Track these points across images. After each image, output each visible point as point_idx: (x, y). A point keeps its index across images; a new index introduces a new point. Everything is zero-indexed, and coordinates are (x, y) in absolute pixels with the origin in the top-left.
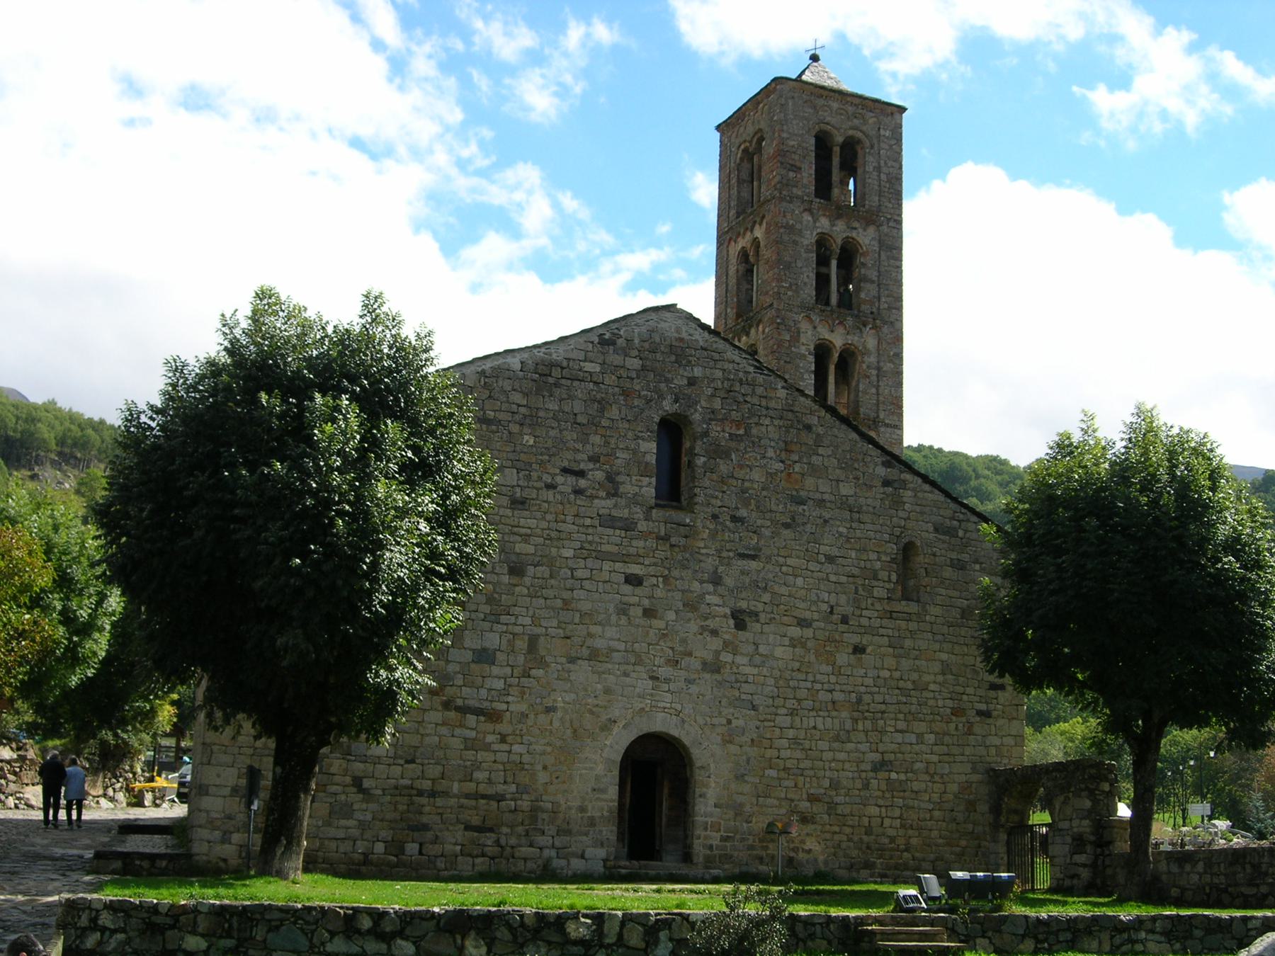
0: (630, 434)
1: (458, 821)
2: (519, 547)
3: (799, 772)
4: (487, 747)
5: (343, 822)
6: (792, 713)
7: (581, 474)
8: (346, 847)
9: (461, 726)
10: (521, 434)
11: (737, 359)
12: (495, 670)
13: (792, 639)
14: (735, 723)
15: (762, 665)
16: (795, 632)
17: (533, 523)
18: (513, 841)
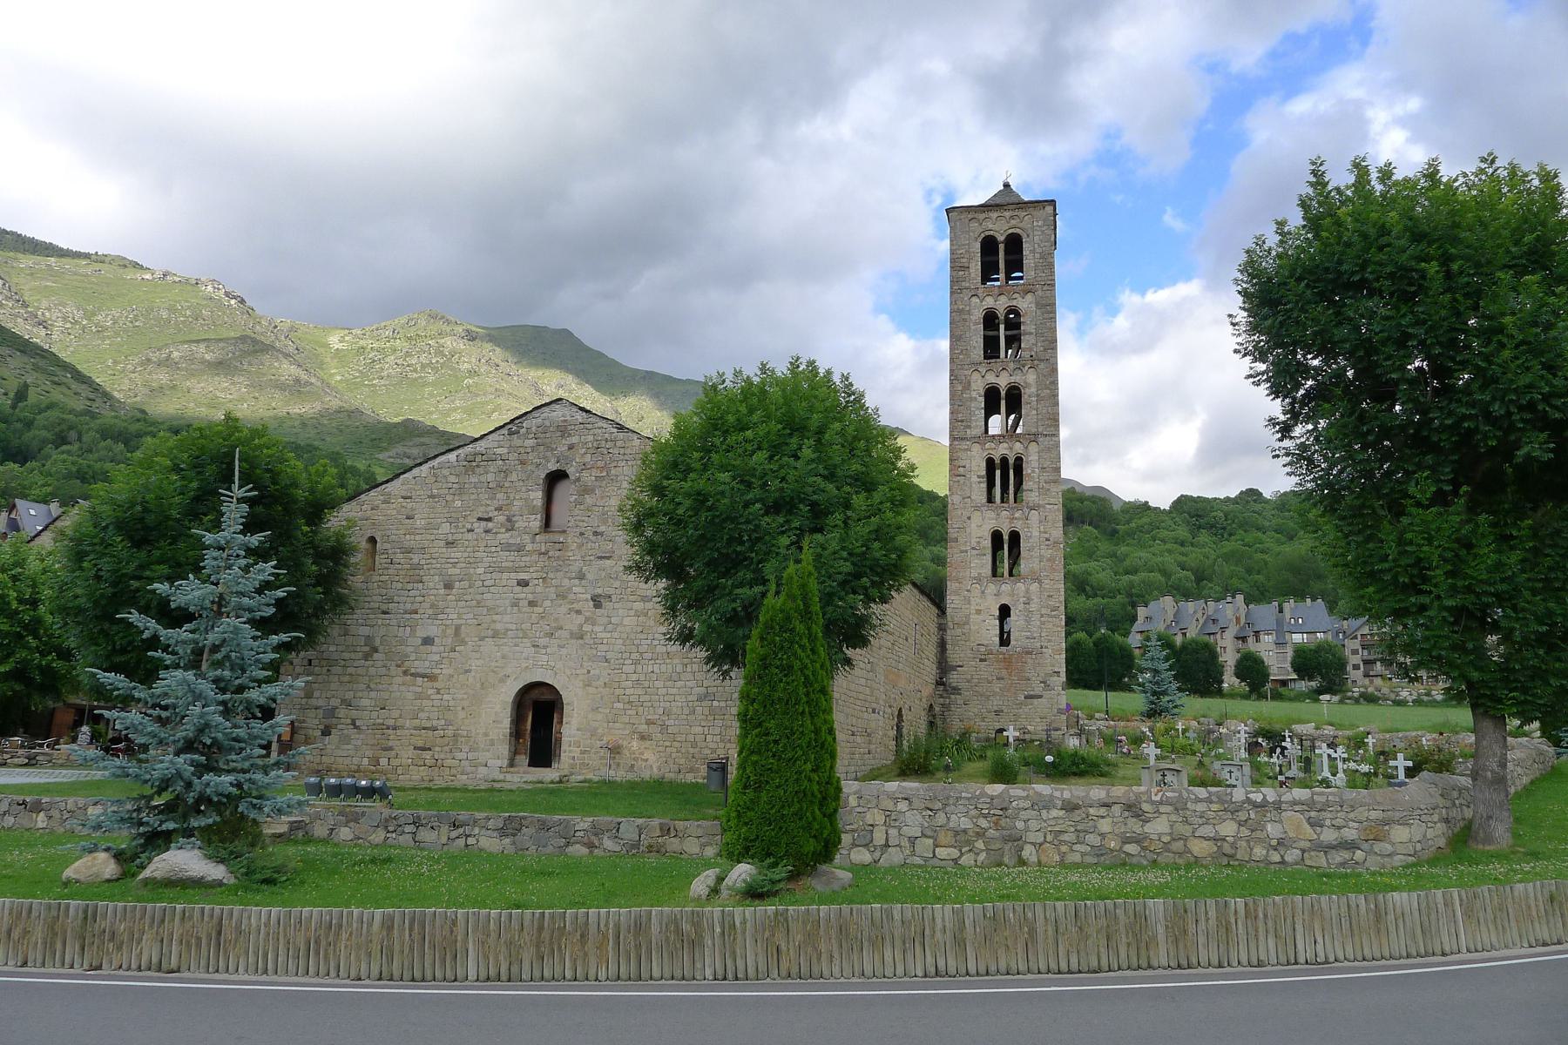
0: (524, 489)
1: (410, 744)
2: (450, 571)
4: (428, 698)
7: (489, 520)
8: (348, 761)
11: (605, 426)
12: (434, 649)
15: (614, 630)
16: (639, 606)
18: (442, 756)
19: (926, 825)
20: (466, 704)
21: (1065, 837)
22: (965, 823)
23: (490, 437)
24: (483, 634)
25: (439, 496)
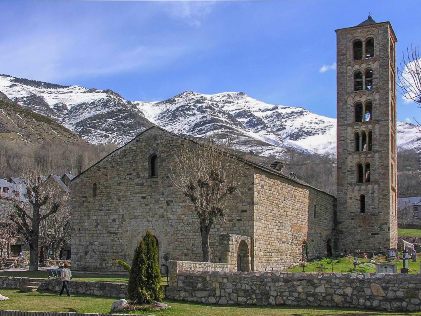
0: (142, 162)
3: (184, 242)
4: (115, 241)
5: (92, 259)
6: (182, 226)
7: (131, 174)
9: (111, 237)
10: (119, 168)
11: (169, 135)
13: (181, 206)
14: (168, 230)
16: (182, 204)
17: (121, 188)
19: (234, 288)
20: (127, 243)
21: (285, 294)
22: (248, 287)
23: (131, 143)
24: (131, 217)
25: (114, 167)
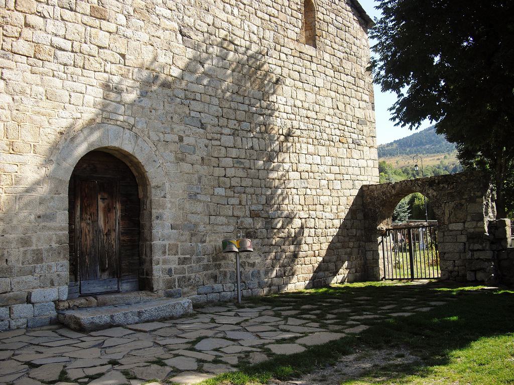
6: (235, 132)
14: (186, 140)
